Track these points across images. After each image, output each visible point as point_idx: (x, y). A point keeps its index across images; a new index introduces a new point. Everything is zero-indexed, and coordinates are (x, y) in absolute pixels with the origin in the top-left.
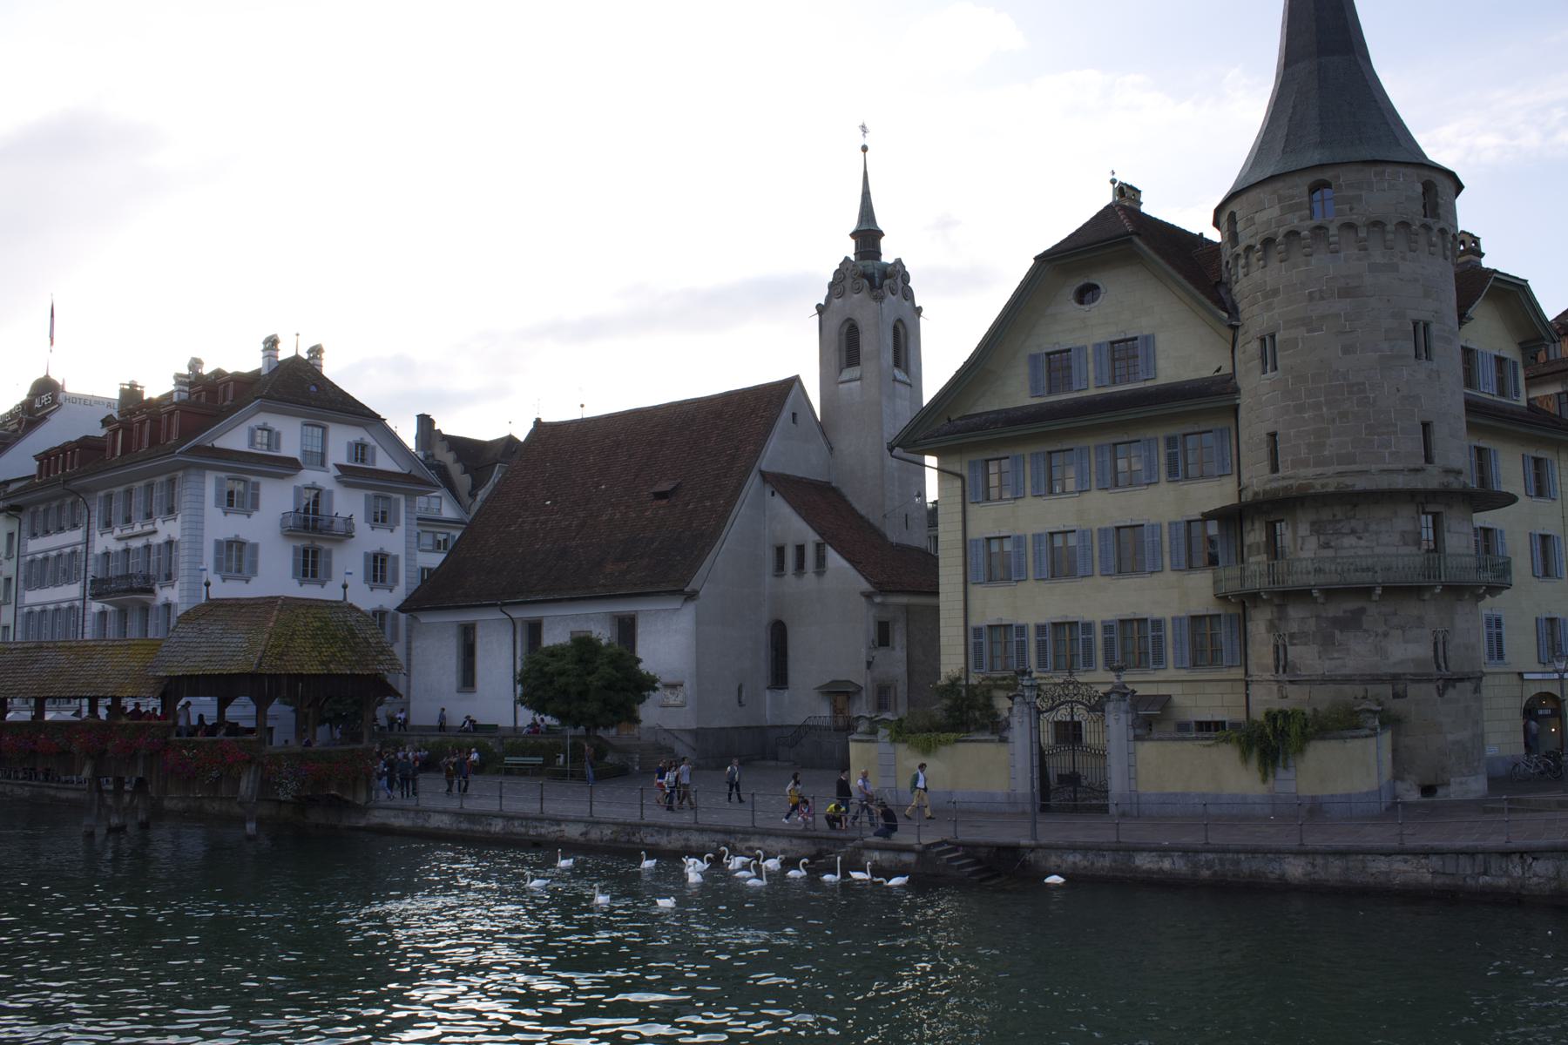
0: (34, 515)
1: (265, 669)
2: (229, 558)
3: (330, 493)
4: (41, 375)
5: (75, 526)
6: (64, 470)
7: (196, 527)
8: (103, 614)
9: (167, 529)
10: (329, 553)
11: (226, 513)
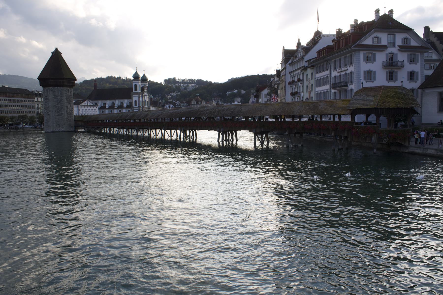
0: (317, 67)
1: (379, 107)
2: (368, 76)
3: (397, 54)
4: (316, 30)
5: (327, 70)
6: (323, 55)
7: (358, 67)
8: (335, 93)
9: (351, 69)
10: (397, 72)
11: (366, 63)
